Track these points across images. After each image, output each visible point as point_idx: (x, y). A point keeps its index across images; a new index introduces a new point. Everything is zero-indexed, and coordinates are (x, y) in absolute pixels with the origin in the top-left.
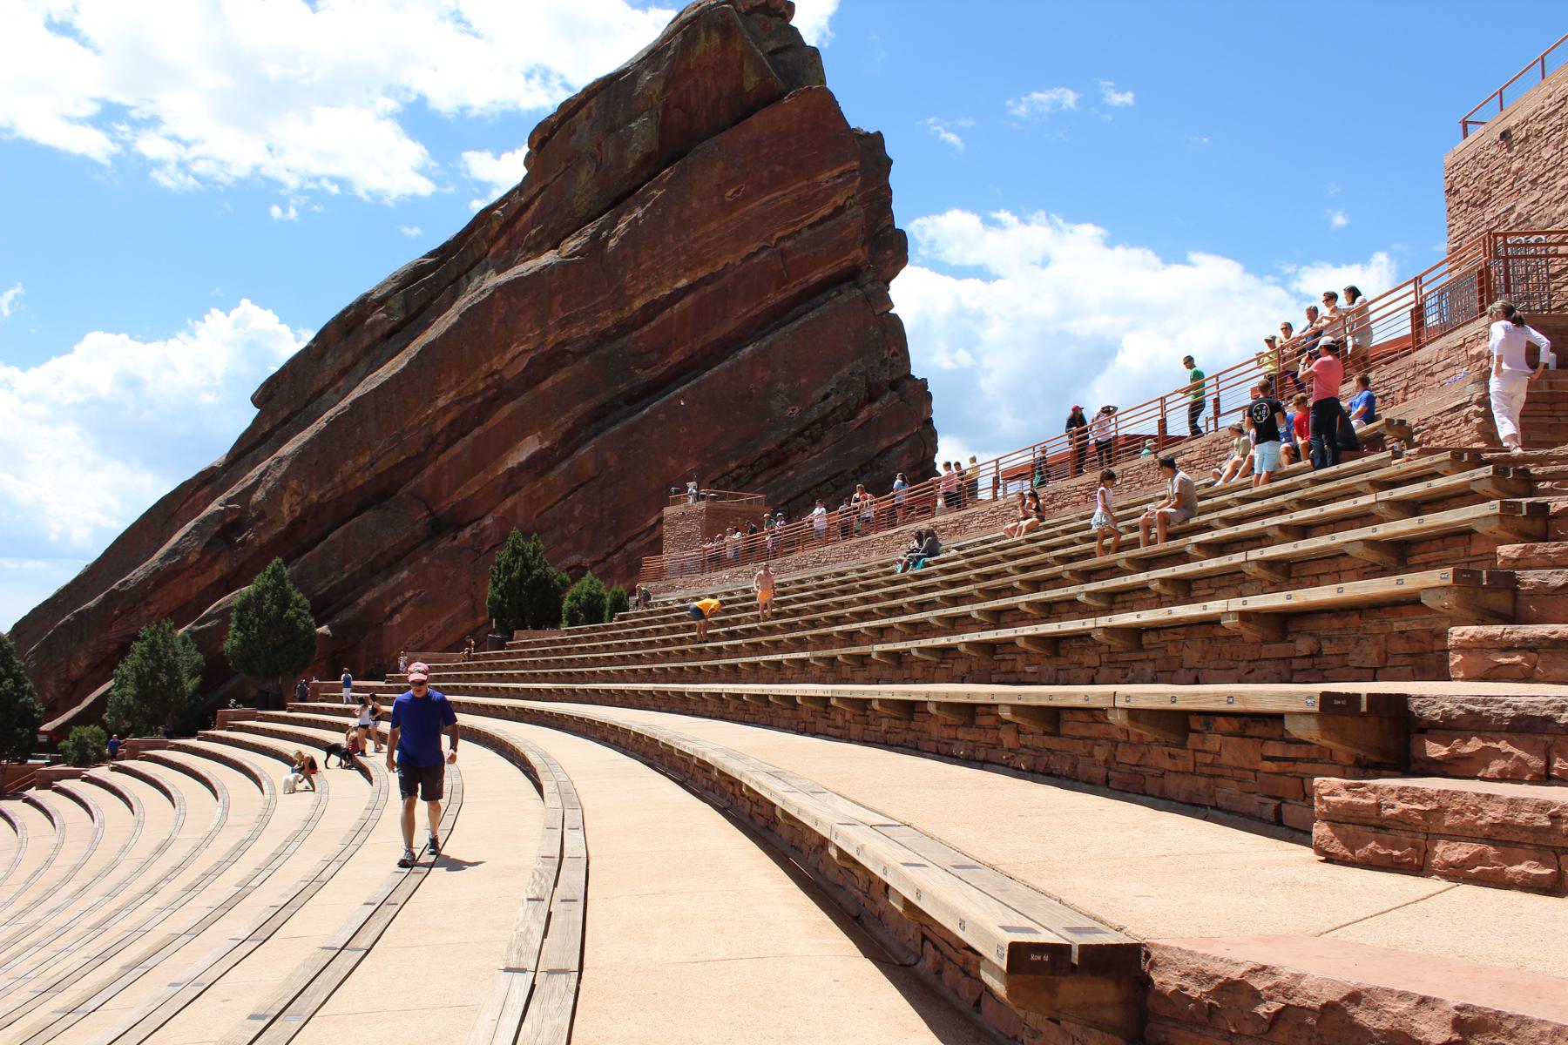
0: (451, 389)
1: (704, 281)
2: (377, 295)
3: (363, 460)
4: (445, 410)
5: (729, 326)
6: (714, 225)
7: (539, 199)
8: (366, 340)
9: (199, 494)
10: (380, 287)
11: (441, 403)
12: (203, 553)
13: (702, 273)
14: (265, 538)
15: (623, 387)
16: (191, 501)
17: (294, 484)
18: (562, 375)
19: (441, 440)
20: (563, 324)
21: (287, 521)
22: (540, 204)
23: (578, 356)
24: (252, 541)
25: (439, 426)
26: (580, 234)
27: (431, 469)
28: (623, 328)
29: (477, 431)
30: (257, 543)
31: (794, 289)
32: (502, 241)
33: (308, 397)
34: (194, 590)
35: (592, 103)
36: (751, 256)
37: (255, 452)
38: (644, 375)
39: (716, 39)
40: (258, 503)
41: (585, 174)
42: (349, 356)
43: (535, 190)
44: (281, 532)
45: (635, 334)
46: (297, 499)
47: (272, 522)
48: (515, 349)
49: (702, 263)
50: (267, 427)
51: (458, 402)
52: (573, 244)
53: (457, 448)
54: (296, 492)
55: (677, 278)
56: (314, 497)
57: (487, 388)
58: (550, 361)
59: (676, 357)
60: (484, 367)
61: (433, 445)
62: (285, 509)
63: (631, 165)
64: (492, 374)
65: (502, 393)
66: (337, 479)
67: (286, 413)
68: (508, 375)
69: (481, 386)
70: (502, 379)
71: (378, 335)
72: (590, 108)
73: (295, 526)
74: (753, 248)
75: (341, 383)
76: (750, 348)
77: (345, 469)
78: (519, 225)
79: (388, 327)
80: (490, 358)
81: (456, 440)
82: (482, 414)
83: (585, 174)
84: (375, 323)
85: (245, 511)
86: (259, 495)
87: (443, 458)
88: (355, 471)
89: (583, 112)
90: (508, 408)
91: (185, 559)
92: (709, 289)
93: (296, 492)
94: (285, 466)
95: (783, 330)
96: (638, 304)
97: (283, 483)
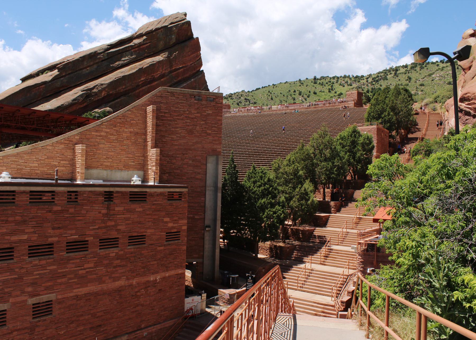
0: (144, 77)
1: (185, 67)
2: (99, 52)
3: (124, 87)
4: (142, 81)
5: (187, 75)
6: (187, 58)
7: (149, 44)
8: (97, 61)
9: (41, 87)
10: (99, 50)
11: (142, 79)
12: (82, 101)
13: (184, 65)
14: (96, 99)
15: (173, 82)
16: (38, 88)
17: (107, 89)
18: (165, 79)
19: (140, 86)
20: (165, 70)
21: (103, 96)
22: (149, 45)
23: (167, 76)
24: (93, 99)
25: (140, 83)
26: (165, 54)
27: (138, 91)
28: (171, 72)
29: (149, 86)
30: (94, 100)
31: (195, 71)
32: (136, 49)
33: (77, 69)
34: (78, 108)
35: (162, 29)
36: (191, 64)
37: (62, 79)
38: (175, 81)
39: (187, 26)
40: (95, 92)
41: (161, 43)
42: (92, 63)
43: (148, 42)
44: (100, 99)
45: (173, 73)
46: (107, 92)
47: (99, 96)
48: (159, 72)
49: (185, 64)
50: (64, 74)
51: (144, 80)
52: (164, 56)
53: (144, 88)
54: (106, 91)
55: (180, 65)
56: (111, 92)
57: (151, 78)
58: (163, 76)
59: (180, 78)
60: (152, 75)
61: (138, 87)
62: (103, 94)
63: (171, 43)
64: (153, 76)
65: (153, 80)
66: (117, 90)
67: (70, 72)
68: (156, 77)
69: (150, 78)
70: (154, 77)
71: (101, 60)
72: (162, 31)
73: (104, 98)
74: (192, 63)
75: (88, 68)
76: (193, 80)
77: (120, 88)
78: (141, 47)
79: (103, 59)
80: (154, 73)
81: (143, 86)
82: (150, 82)
83: (161, 43)
84: (100, 58)
85: (91, 93)
86: (95, 90)
87: (141, 89)
88: (121, 89)
89: (160, 31)
90: (156, 83)
91: (79, 101)
92: (185, 68)
93: (106, 91)
94: (104, 86)
95: (197, 78)
96: (174, 68)
97: (104, 89)
